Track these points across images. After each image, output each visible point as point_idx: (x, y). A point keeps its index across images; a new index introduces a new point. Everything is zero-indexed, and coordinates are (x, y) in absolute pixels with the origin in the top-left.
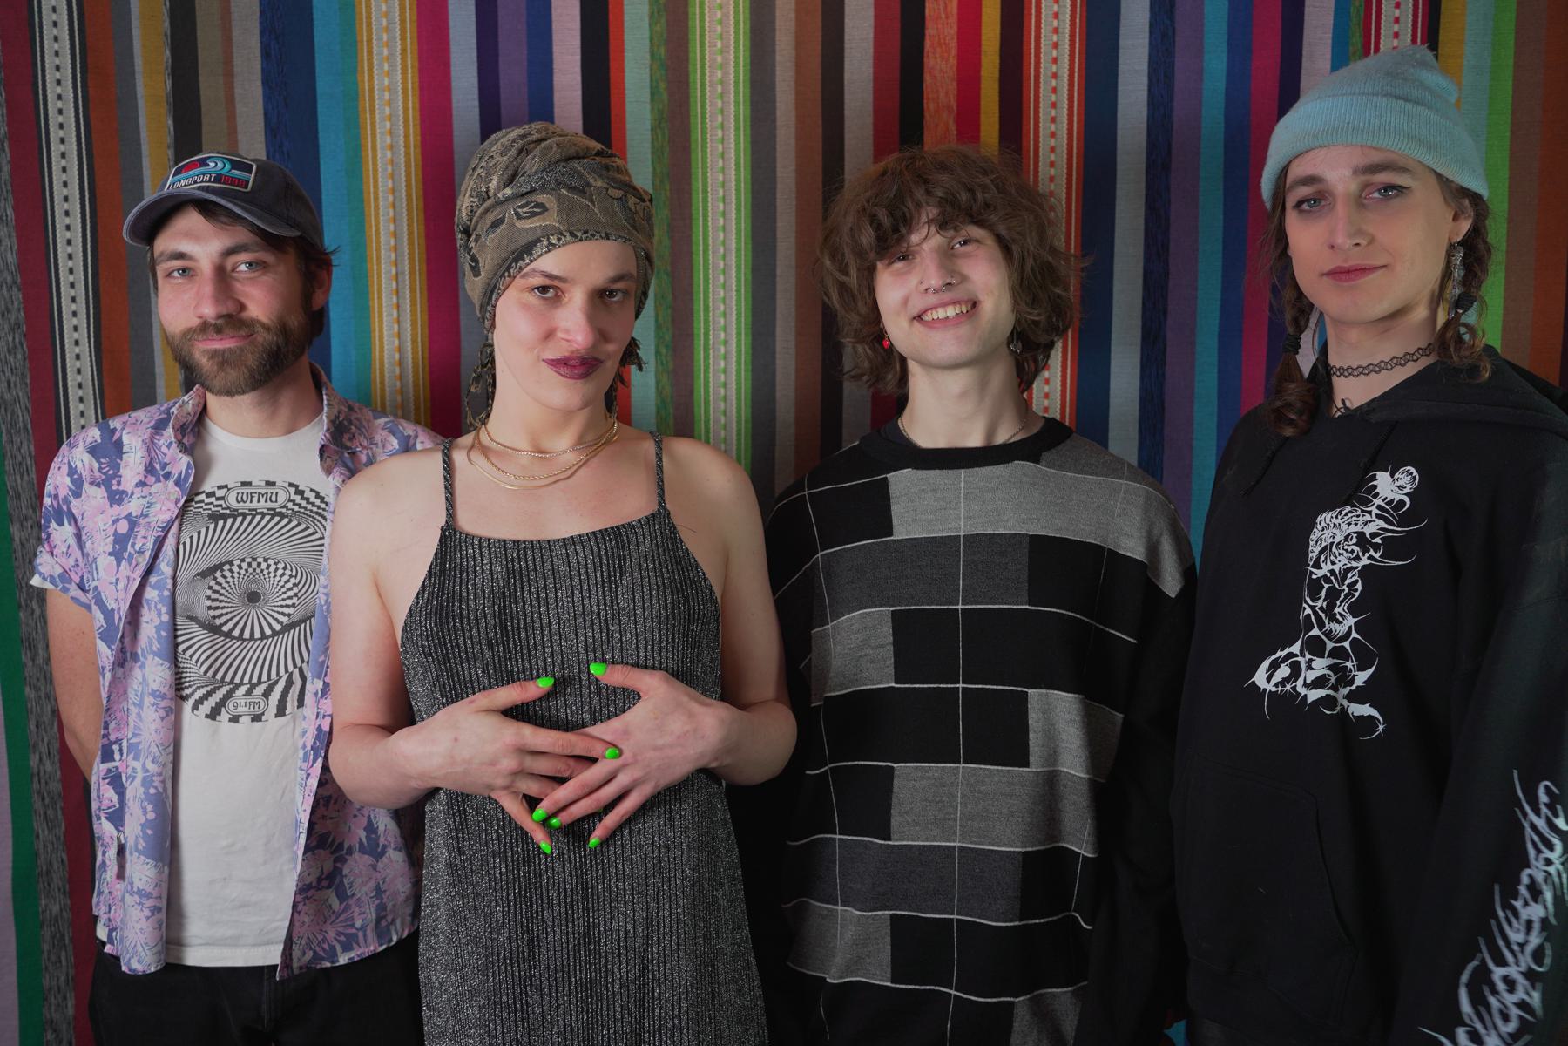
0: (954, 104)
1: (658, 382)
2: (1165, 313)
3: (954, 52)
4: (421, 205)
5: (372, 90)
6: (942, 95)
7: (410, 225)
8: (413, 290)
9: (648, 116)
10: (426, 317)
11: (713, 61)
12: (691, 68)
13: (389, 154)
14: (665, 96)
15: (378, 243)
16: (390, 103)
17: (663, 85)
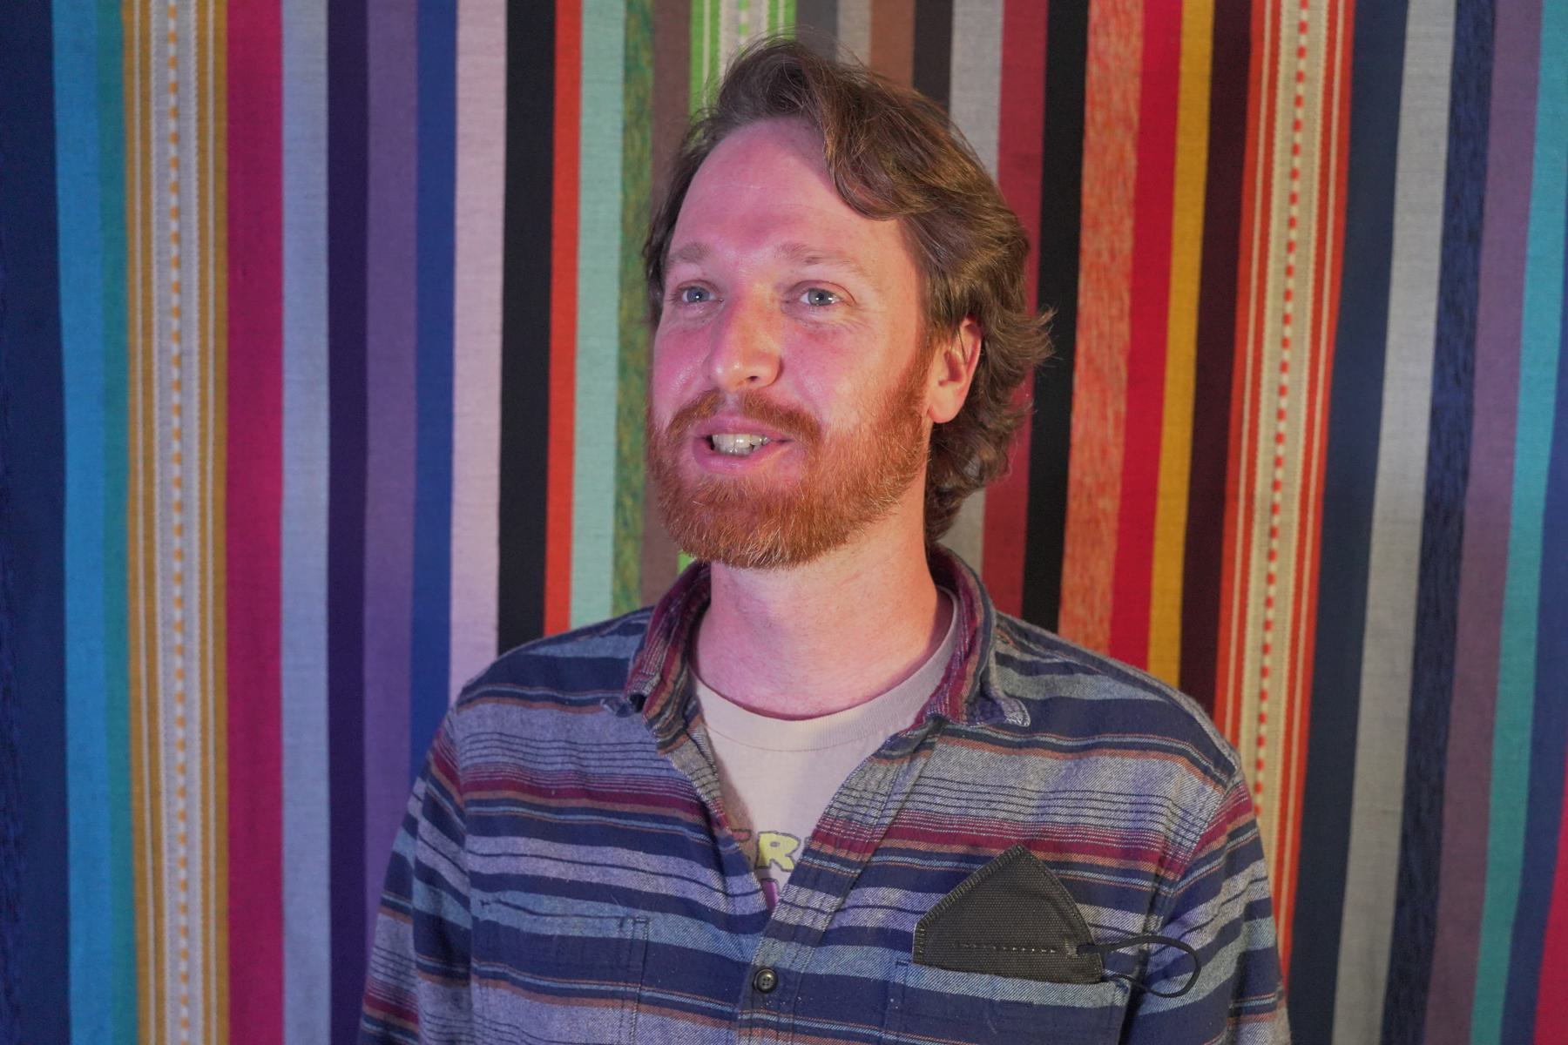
0: (1135, 116)
1: (617, 556)
2: (1465, 473)
3: (1138, 26)
4: (223, 236)
5: (145, 39)
6: (1116, 97)
7: (203, 273)
8: (203, 386)
9: (619, 105)
10: (223, 430)
11: (736, 19)
12: (694, 29)
13: (173, 151)
14: (649, 74)
15: (147, 299)
16: (175, 62)
17: (645, 57)
